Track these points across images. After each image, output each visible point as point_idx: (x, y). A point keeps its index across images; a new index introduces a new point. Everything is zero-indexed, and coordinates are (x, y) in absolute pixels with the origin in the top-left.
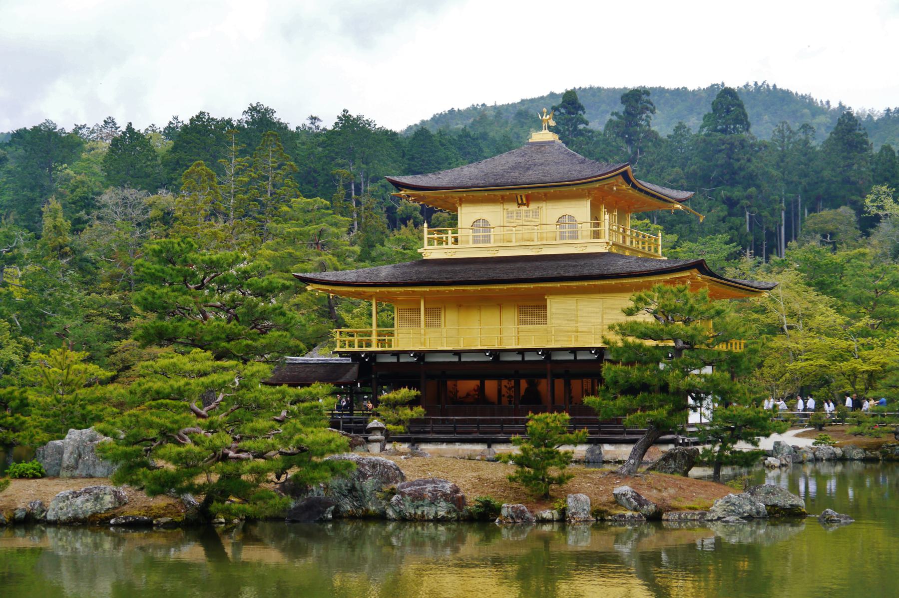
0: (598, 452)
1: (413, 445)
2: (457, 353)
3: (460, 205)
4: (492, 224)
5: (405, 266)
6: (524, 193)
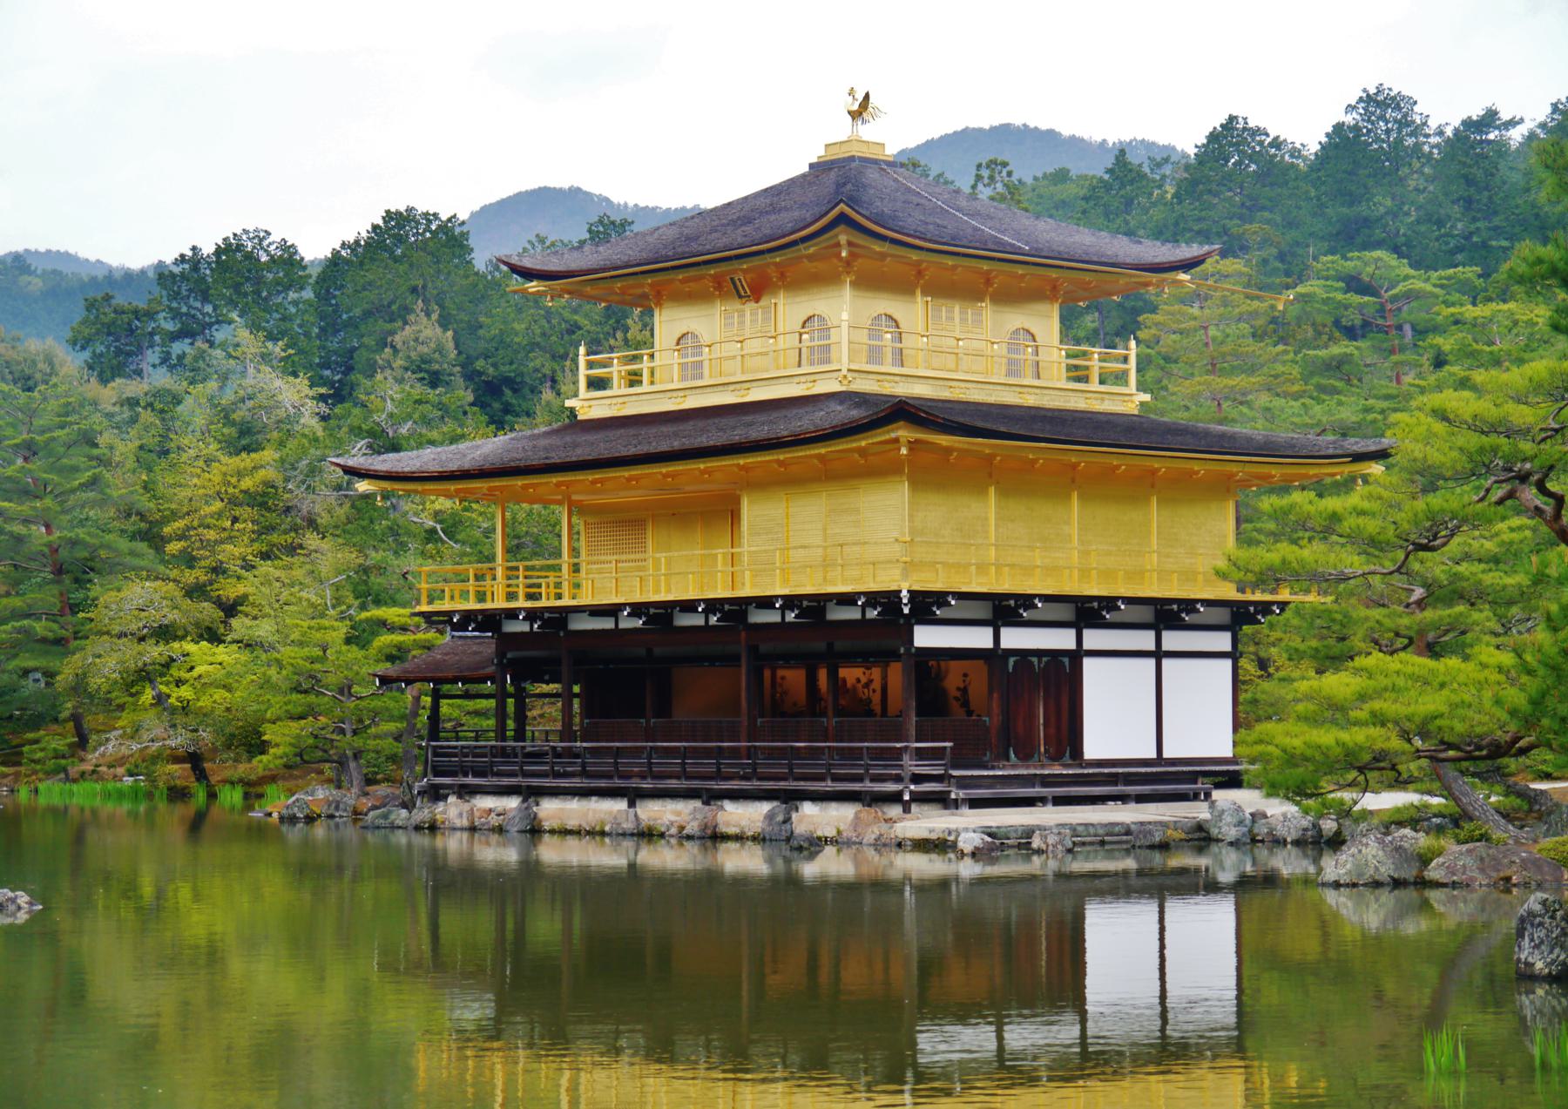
0: (780, 818)
1: (524, 801)
2: (612, 611)
3: (659, 304)
4: (706, 338)
5: (538, 436)
6: (742, 272)
